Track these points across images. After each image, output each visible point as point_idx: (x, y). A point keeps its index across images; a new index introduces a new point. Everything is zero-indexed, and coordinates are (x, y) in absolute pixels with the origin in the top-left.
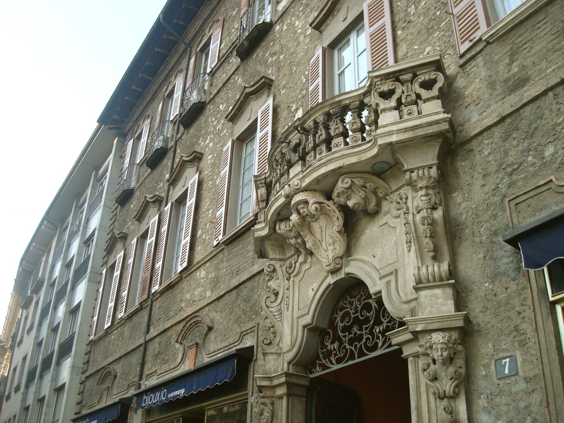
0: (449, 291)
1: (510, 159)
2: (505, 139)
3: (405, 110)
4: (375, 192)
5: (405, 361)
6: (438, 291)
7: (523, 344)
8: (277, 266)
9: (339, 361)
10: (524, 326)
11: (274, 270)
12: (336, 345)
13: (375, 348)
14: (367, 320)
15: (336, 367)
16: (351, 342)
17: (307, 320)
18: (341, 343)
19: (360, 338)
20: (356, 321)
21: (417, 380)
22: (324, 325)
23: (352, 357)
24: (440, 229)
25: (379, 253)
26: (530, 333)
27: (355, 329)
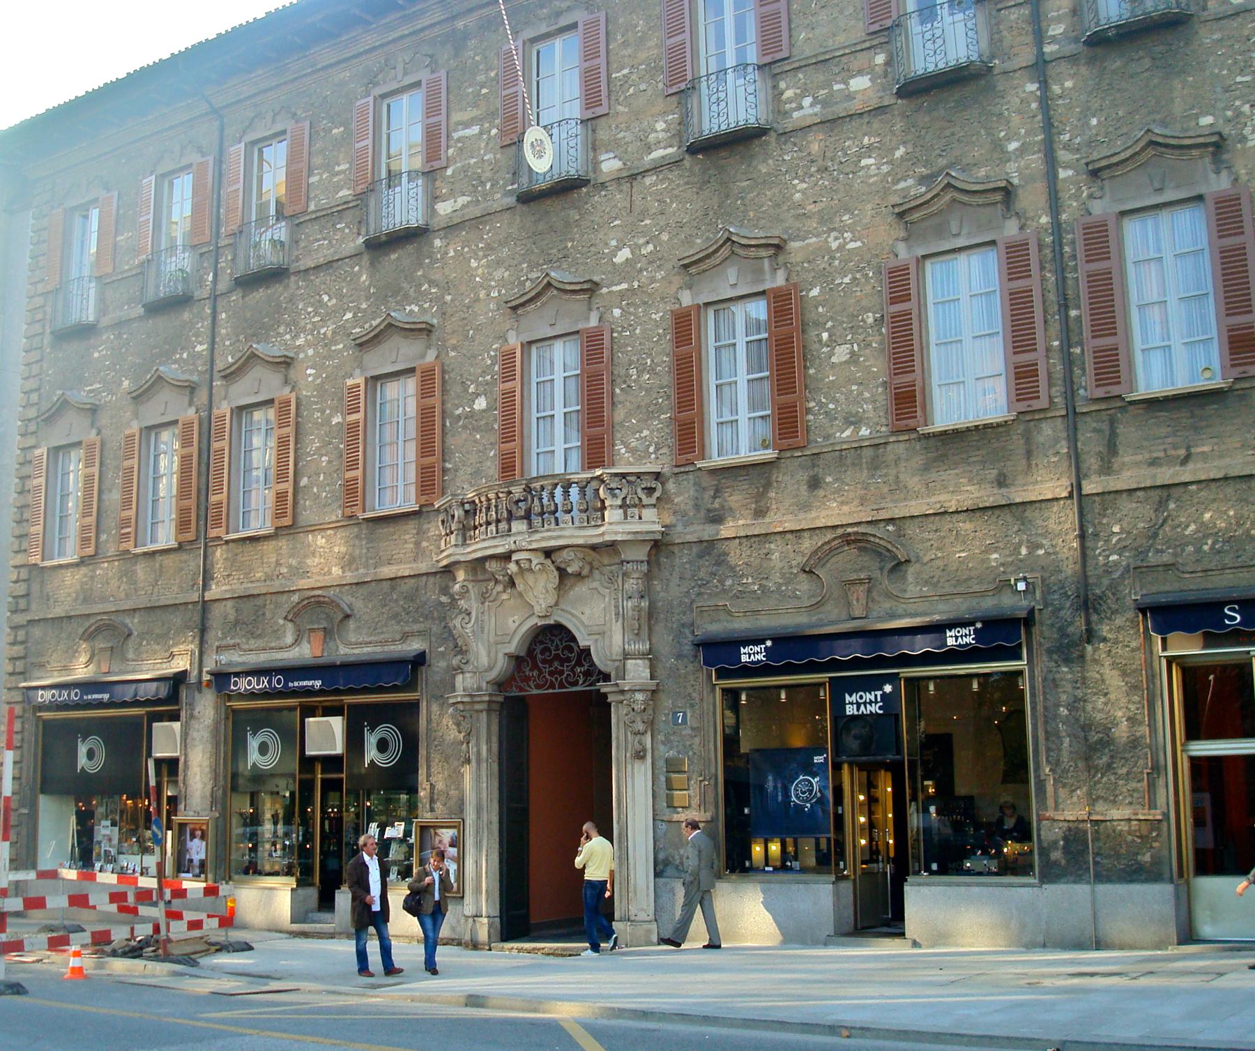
0: (647, 662)
1: (702, 575)
2: (700, 557)
3: (630, 511)
4: (591, 564)
5: (610, 705)
6: (639, 661)
7: (692, 706)
8: (470, 587)
9: (538, 687)
10: (694, 695)
11: (468, 591)
12: (535, 673)
13: (576, 683)
14: (568, 660)
15: (535, 692)
16: (551, 674)
17: (512, 648)
18: (541, 673)
19: (561, 673)
20: (557, 657)
21: (617, 717)
22: (522, 654)
23: (552, 686)
24: (644, 614)
25: (587, 612)
26: (697, 700)
27: (556, 664)
